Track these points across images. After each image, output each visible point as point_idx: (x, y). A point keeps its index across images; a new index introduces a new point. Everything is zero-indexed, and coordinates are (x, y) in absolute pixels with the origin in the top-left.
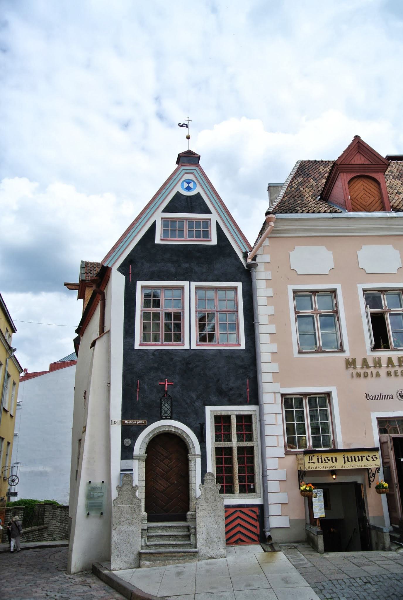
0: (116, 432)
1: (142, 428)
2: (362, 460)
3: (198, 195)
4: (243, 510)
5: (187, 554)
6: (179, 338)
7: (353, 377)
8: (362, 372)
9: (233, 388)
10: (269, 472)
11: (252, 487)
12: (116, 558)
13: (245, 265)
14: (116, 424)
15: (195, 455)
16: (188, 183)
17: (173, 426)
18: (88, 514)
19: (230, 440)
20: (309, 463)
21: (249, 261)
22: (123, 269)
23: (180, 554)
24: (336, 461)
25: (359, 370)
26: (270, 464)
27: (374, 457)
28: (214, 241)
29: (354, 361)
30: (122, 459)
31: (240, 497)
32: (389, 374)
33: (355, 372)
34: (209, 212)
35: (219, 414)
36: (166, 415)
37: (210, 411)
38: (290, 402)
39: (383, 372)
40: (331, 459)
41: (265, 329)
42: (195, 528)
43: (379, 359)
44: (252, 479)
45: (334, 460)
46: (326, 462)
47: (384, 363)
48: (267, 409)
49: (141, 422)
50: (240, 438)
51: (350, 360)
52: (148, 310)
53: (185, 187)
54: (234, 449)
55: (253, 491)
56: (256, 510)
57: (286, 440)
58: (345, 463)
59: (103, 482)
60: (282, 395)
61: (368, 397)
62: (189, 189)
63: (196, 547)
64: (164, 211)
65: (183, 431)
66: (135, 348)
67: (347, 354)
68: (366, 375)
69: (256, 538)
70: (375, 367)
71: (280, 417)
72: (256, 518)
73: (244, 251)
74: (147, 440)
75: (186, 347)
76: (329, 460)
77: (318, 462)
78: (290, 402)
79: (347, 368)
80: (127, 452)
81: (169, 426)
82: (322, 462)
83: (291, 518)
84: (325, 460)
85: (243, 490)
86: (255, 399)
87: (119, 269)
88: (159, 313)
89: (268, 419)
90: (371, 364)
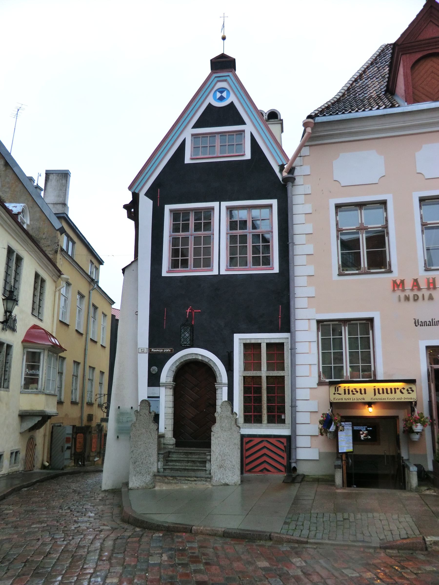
1: (169, 356)
2: (395, 393)
3: (232, 104)
4: (270, 440)
5: (199, 479)
6: (208, 263)
7: (400, 300)
8: (411, 295)
10: (299, 403)
11: (283, 417)
12: (134, 478)
13: (281, 180)
14: (143, 352)
15: (221, 384)
16: (221, 92)
17: (200, 355)
18: (118, 437)
19: (260, 369)
20: (334, 394)
21: (285, 174)
23: (192, 479)
24: (365, 393)
25: (408, 293)
26: (300, 394)
27: (409, 389)
28: (248, 156)
29: (402, 282)
30: (149, 386)
31: (268, 428)
33: (402, 295)
34: (243, 123)
35: (248, 342)
36: (185, 343)
37: (239, 339)
38: (329, 329)
40: (359, 391)
41: (301, 248)
42: (210, 455)
43: (434, 279)
44: (282, 410)
45: (363, 392)
46: (354, 394)
48: (300, 336)
49: (168, 350)
50: (270, 367)
51: (398, 282)
52: (234, 232)
53: (218, 97)
54: (262, 378)
55: (283, 421)
56: (284, 440)
57: (321, 370)
58: (375, 394)
59: (132, 408)
60: (319, 322)
61: (417, 323)
62: (222, 99)
63: (210, 474)
64: (195, 127)
65: (211, 360)
66: (163, 275)
67: (396, 275)
69: (282, 468)
70: (429, 289)
71: (314, 346)
72: (283, 448)
73: (280, 163)
74: (174, 368)
75: (215, 272)
76: (357, 392)
77: (345, 393)
78: (329, 329)
79: (394, 290)
80: (154, 380)
81: (197, 354)
82: (349, 393)
83: (321, 451)
84: (352, 391)
85: (271, 420)
86: (285, 325)
87: (146, 194)
88: (246, 235)
89: (300, 348)
90: (423, 285)
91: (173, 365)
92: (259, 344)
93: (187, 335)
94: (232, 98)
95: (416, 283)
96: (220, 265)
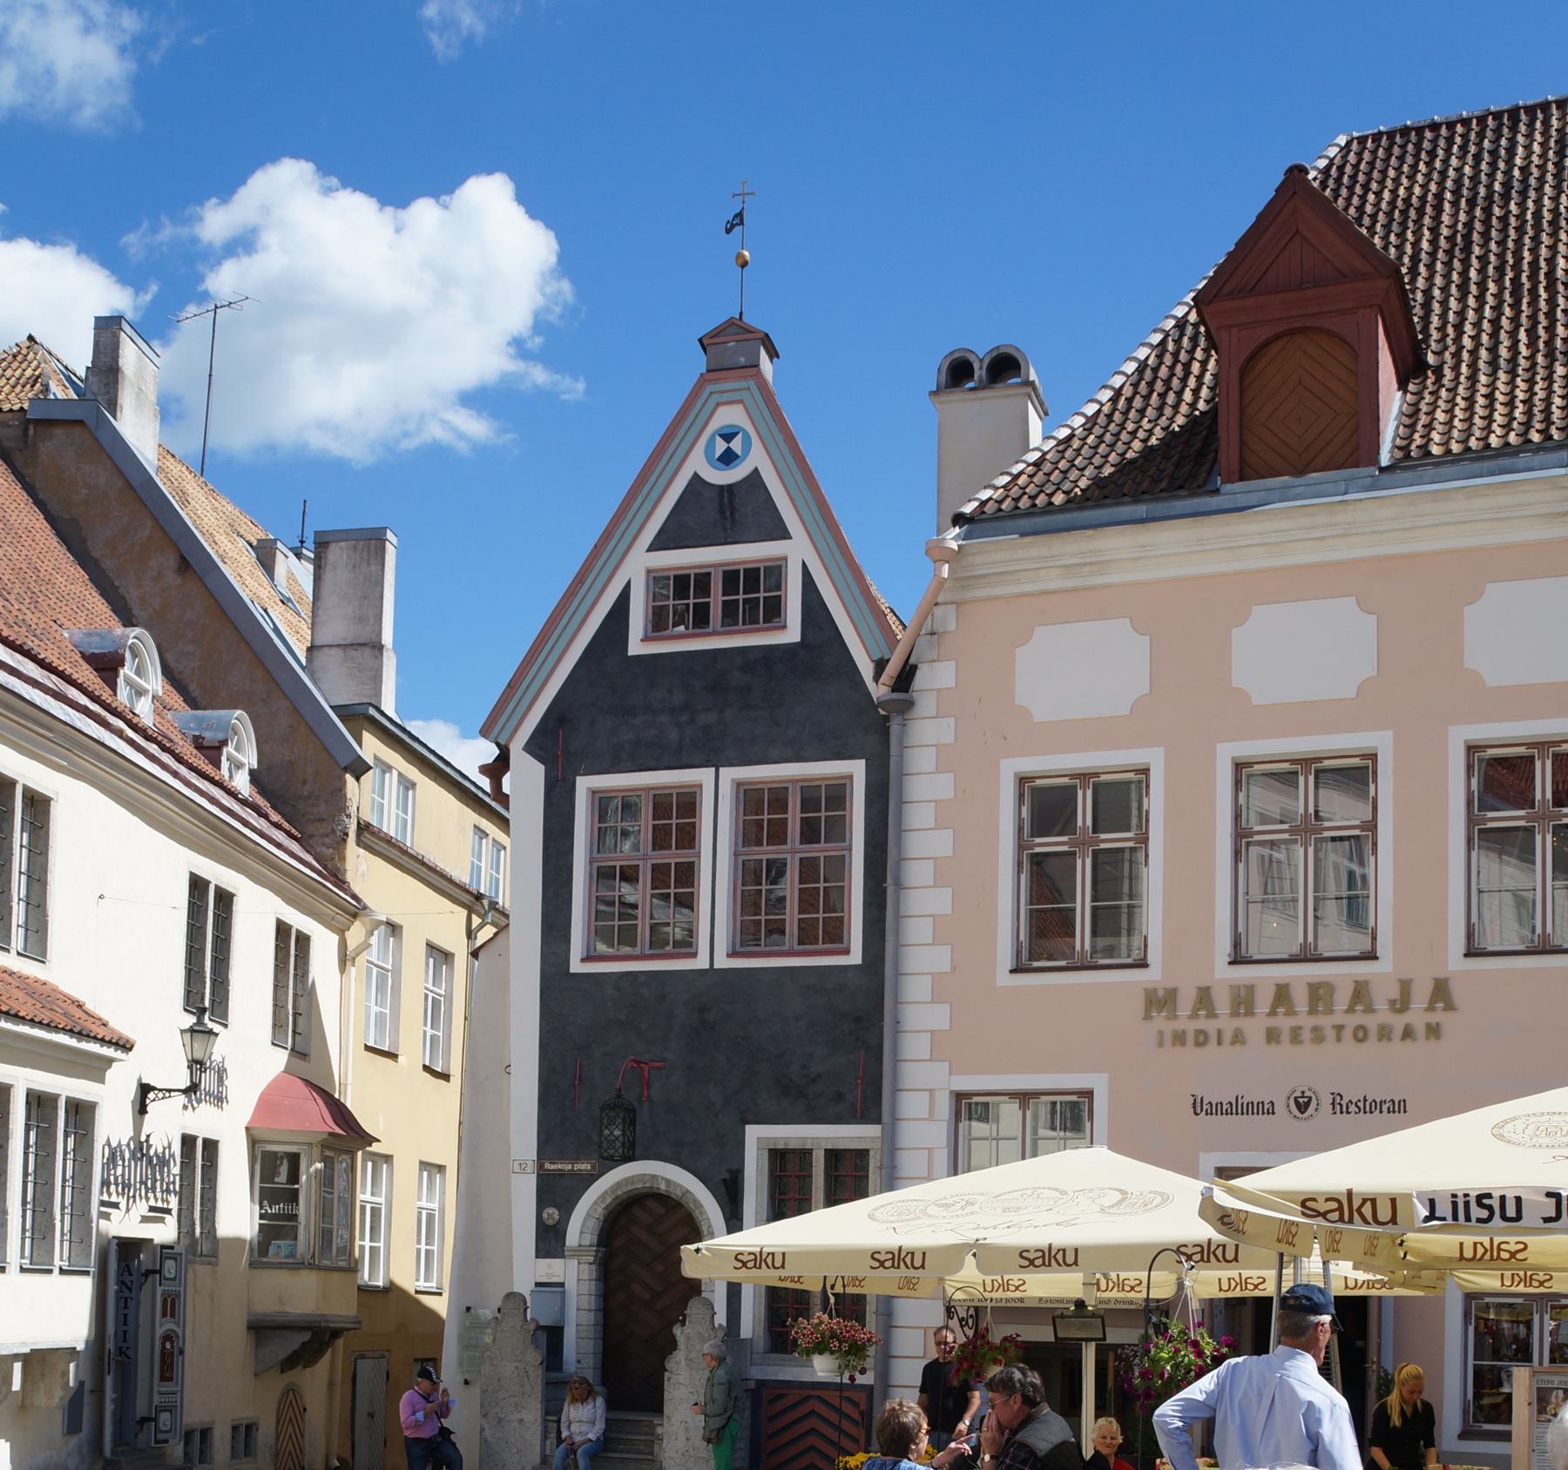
0: (525, 1189)
7: (1161, 1045)
8: (1190, 1027)
9: (819, 1076)
14: (523, 1171)
16: (728, 437)
22: (533, 747)
28: (792, 633)
32: (1272, 1036)
34: (784, 534)
37: (758, 1137)
39: (1255, 1027)
43: (1251, 989)
47: (1264, 1001)
49: (584, 1166)
51: (1161, 993)
53: (718, 454)
61: (1198, 1106)
62: (728, 458)
64: (658, 545)
66: (572, 970)
67: (1152, 975)
68: (1201, 1039)
70: (1235, 1014)
73: (877, 656)
80: (550, 1240)
91: (595, 1203)
92: (809, 1152)
93: (617, 1133)
94: (757, 459)
95: (1204, 997)
96: (714, 943)
